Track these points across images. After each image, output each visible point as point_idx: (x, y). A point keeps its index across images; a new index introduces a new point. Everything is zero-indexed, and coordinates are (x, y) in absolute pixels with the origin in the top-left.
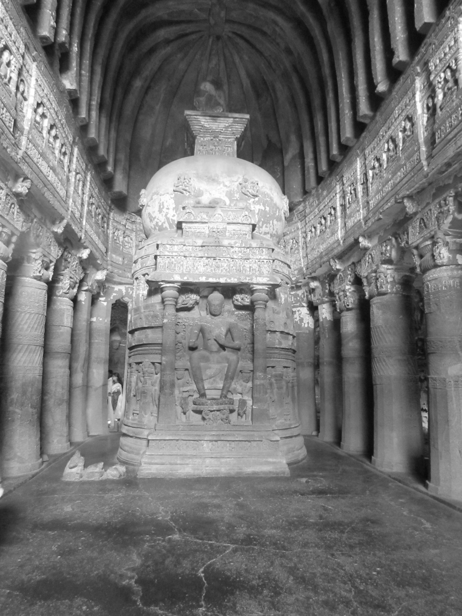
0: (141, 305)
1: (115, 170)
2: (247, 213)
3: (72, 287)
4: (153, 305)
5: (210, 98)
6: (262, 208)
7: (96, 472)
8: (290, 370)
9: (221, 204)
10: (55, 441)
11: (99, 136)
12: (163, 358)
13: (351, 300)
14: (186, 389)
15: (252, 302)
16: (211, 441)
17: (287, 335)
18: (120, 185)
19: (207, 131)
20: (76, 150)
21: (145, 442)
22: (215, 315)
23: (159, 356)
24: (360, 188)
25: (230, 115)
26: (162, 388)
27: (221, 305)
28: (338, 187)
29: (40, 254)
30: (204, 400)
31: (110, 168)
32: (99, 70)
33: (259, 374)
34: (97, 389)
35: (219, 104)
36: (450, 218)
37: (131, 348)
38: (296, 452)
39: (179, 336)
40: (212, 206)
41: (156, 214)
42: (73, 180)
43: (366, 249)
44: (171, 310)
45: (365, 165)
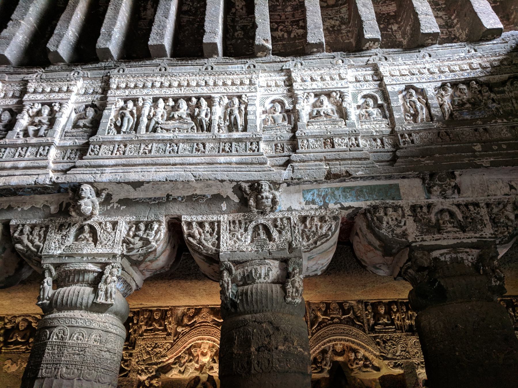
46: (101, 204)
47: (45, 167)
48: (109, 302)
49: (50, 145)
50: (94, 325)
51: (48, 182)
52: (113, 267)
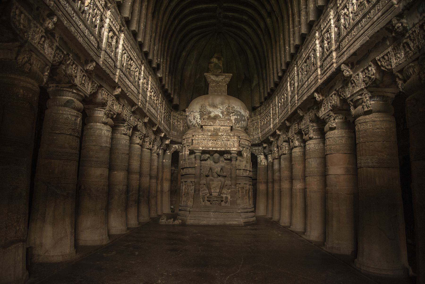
0: (187, 158)
1: (174, 96)
3: (157, 149)
4: (191, 158)
5: (216, 64)
7: (171, 221)
8: (247, 185)
9: (219, 117)
11: (169, 87)
13: (277, 154)
15: (231, 158)
18: (176, 101)
19: (214, 81)
20: (160, 95)
21: (188, 212)
24: (277, 109)
26: (195, 192)
27: (219, 159)
28: (271, 105)
29: (148, 140)
31: (172, 96)
32: (169, 59)
34: (165, 193)
37: (182, 175)
39: (202, 171)
40: (216, 117)
41: (192, 120)
43: (279, 135)
44: (198, 161)
46: (351, 69)
47: (333, 64)
49: (331, 52)
50: (367, 120)
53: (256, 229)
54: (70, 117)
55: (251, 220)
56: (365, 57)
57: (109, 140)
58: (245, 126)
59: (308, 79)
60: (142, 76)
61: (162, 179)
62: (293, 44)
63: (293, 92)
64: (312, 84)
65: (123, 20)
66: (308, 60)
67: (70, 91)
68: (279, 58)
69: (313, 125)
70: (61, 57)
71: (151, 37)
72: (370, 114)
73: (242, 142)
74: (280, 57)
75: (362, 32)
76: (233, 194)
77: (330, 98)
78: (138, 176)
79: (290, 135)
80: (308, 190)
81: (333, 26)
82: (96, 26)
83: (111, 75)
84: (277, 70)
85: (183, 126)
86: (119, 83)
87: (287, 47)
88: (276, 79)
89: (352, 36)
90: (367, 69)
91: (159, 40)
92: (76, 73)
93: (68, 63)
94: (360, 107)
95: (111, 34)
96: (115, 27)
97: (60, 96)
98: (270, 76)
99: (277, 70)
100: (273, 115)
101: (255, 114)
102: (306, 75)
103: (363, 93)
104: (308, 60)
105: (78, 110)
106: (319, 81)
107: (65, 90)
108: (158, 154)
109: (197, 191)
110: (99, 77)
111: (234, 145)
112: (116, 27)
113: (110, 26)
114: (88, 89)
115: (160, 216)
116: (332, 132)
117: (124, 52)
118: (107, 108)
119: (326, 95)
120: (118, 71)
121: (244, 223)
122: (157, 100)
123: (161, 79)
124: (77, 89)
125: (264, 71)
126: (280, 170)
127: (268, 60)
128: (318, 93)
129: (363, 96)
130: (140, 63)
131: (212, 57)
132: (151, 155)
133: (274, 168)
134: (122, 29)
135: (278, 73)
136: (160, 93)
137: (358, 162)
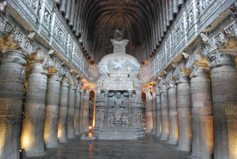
0: (99, 95)
1: (91, 54)
2: (126, 71)
3: (80, 89)
4: (102, 96)
5: (118, 34)
6: (131, 68)
8: (139, 113)
9: (120, 69)
10: (76, 132)
11: (87, 48)
12: (105, 110)
13: (159, 92)
14: (110, 118)
16: (117, 131)
17: (138, 104)
18: (92, 59)
19: (117, 45)
20: (82, 54)
21: (100, 132)
22: (118, 98)
23: (104, 109)
24: (158, 63)
25: (123, 40)
26: (104, 118)
27: (120, 96)
28: (154, 60)
30: (115, 121)
31: (90, 54)
32: (87, 30)
33: (129, 114)
34: (85, 118)
35: (120, 36)
36: (172, 77)
37: (96, 107)
38: (141, 135)
39: (109, 104)
40: (118, 69)
41: (103, 70)
42: (81, 62)
43: (160, 80)
44: (107, 97)
45: (159, 57)
46: (208, 36)
47: (195, 33)
48: (220, 63)
49: (194, 25)
50: (219, 71)
51: (196, 37)
52: (217, 53)
53: (145, 143)
54: (17, 70)
55: (142, 136)
56: (217, 28)
57: (45, 85)
58: (137, 73)
59: (178, 43)
60: (69, 41)
61: (83, 109)
62: (169, 20)
63: (168, 52)
64: (181, 46)
65: (55, 4)
66: (178, 30)
67: (17, 52)
68: (159, 29)
69: (182, 73)
70: (10, 29)
71: (74, 15)
72: (221, 66)
73: (136, 84)
74: (160, 28)
75: (214, 11)
76: (130, 119)
77: (194, 55)
78: (66, 108)
79: (167, 79)
80: (179, 117)
81: (195, 7)
82: (35, 8)
83: (46, 41)
84: (158, 37)
85: (97, 74)
86: (52, 46)
87: (164, 22)
88: (158, 43)
89: (207, 14)
90: (218, 36)
91: (80, 18)
92: (21, 40)
93: (15, 33)
94: (214, 62)
95: (46, 13)
96: (49, 9)
97: (11, 55)
98: (153, 41)
99: (158, 37)
100: (156, 67)
101: (144, 66)
102: (177, 40)
103: (215, 53)
104: (178, 30)
105: (24, 65)
106: (186, 44)
107: (13, 51)
108: (80, 93)
109: (106, 117)
110: (39, 43)
111: (130, 87)
112: (50, 9)
113: (46, 8)
114: (30, 50)
115: (81, 134)
116: (195, 78)
117: (56, 25)
118: (44, 63)
119: (191, 54)
120: (52, 38)
121: (137, 138)
122: (79, 57)
123: (82, 44)
124: (22, 51)
125: (150, 38)
126: (160, 103)
127: (152, 31)
128: (185, 52)
129: (216, 55)
130: (67, 32)
131: (116, 29)
132: (76, 94)
133: (157, 101)
134: (54, 10)
135: (159, 39)
136: (81, 52)
137: (213, 99)
